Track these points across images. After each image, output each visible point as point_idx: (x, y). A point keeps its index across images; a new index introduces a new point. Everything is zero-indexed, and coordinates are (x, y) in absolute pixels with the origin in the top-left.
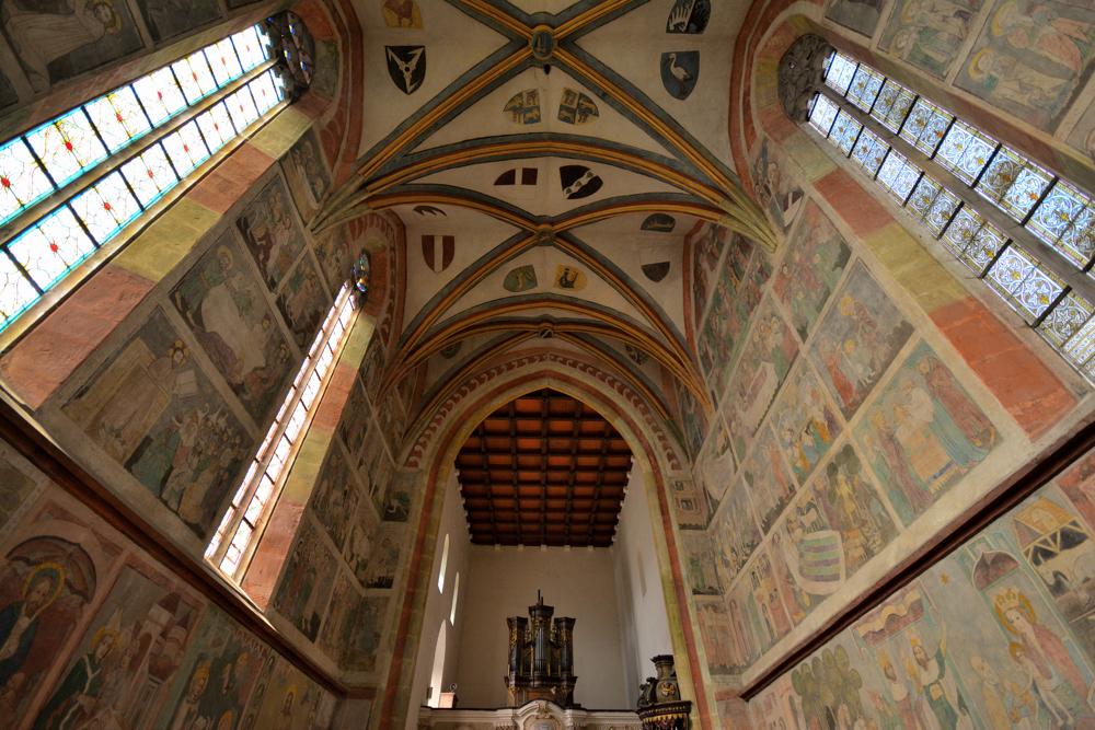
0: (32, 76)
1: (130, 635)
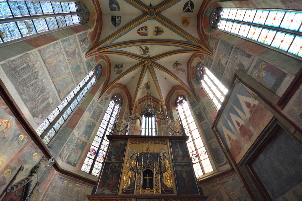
0: (253, 59)
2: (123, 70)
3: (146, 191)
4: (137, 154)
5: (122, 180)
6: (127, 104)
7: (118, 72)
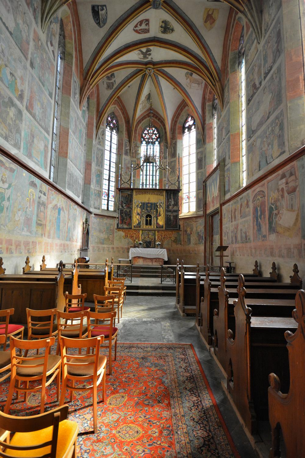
1: (277, 193)
2: (115, 81)
3: (147, 227)
4: (141, 203)
5: (133, 221)
6: (124, 130)
7: (109, 86)
